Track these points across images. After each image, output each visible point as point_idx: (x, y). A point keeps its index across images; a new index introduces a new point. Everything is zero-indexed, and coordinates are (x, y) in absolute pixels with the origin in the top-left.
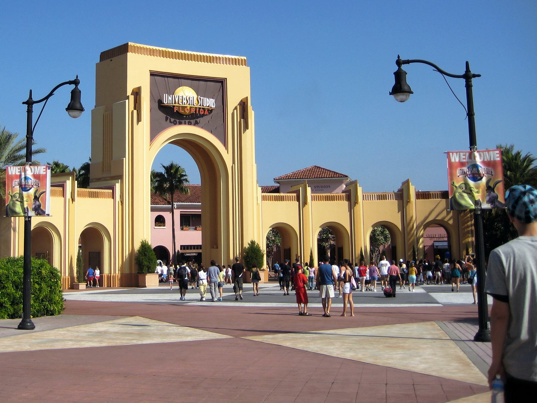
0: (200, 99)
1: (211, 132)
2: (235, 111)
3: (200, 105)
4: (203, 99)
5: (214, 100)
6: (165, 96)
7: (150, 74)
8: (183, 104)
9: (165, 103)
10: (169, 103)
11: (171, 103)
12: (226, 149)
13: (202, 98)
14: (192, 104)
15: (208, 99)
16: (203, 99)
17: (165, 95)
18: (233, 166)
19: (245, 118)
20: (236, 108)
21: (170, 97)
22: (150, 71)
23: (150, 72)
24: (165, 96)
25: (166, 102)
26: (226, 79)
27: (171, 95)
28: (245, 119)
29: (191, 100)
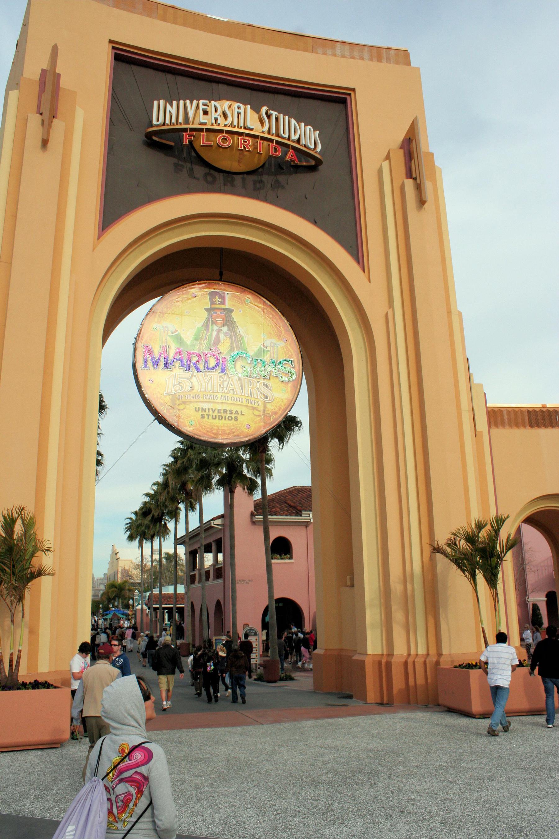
0: (269, 116)
1: (315, 223)
2: (386, 165)
3: (269, 132)
4: (277, 119)
5: (318, 132)
6: (158, 105)
7: (116, 54)
8: (213, 121)
9: (155, 122)
10: (168, 121)
11: (174, 120)
12: (364, 271)
13: (274, 113)
14: (242, 124)
15: (293, 122)
16: (277, 119)
17: (156, 103)
18: (387, 315)
19: (414, 176)
20: (388, 157)
21: (171, 105)
22: (111, 41)
23: (113, 48)
24: (158, 105)
25: (158, 120)
26: (353, 90)
27: (175, 103)
28: (415, 179)
29: (239, 114)
